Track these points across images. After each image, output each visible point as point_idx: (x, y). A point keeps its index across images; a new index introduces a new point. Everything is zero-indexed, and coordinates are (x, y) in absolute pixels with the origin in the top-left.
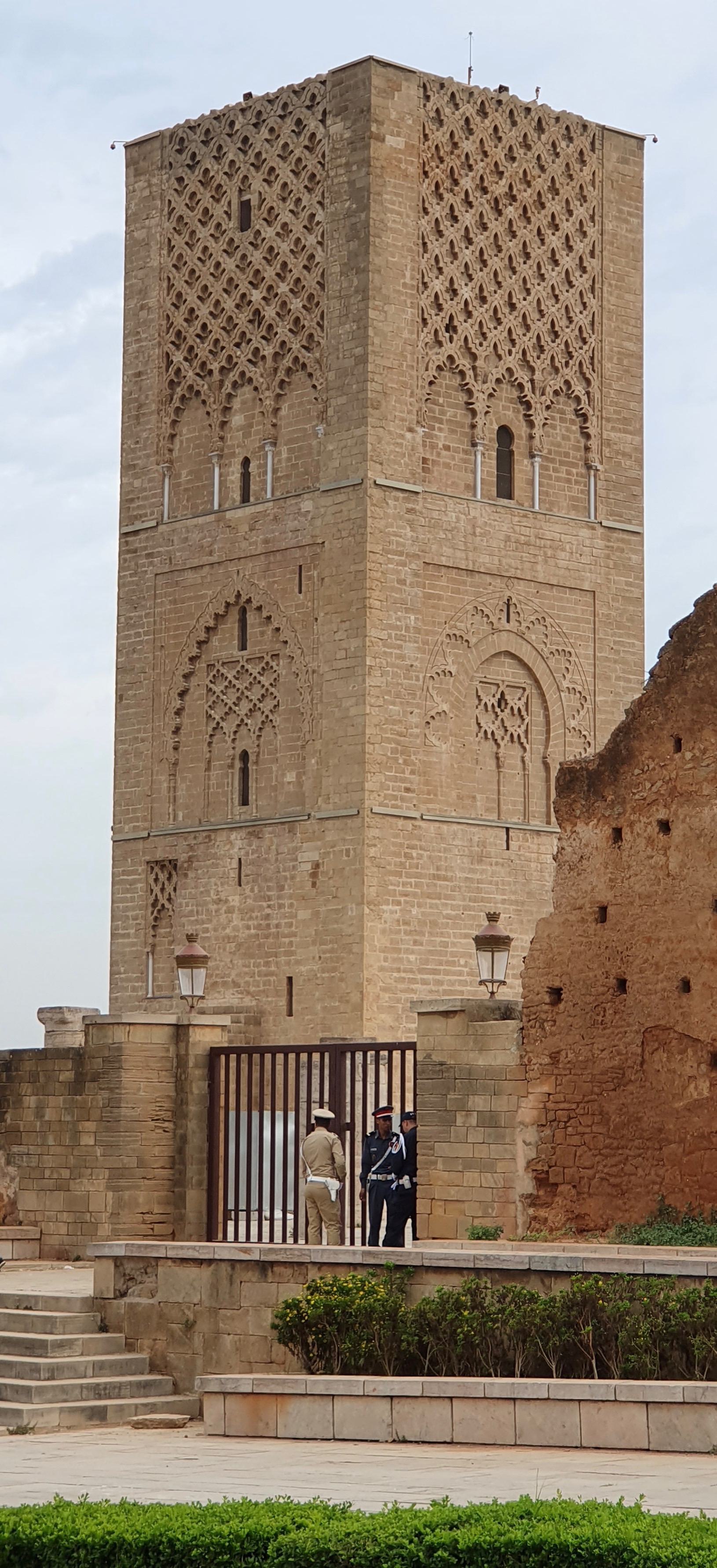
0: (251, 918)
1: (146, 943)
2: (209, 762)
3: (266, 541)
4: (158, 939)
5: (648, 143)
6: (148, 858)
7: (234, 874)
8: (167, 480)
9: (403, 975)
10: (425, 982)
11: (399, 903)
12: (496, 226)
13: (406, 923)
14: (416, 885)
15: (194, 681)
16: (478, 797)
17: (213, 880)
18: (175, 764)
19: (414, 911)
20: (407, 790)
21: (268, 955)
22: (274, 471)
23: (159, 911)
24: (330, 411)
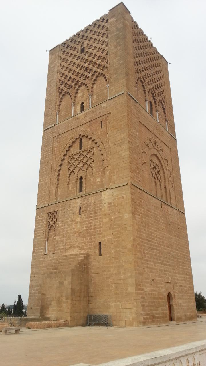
0: (84, 224)
1: (45, 237)
2: (69, 182)
3: (90, 118)
4: (50, 236)
5: (168, 64)
6: (47, 212)
7: (78, 212)
8: (57, 115)
9: (142, 240)
11: (140, 216)
13: (142, 223)
15: (64, 161)
16: (153, 192)
17: (70, 215)
18: (58, 184)
19: (144, 219)
20: (140, 181)
21: (91, 236)
22: (92, 102)
23: (51, 227)
24: (111, 80)
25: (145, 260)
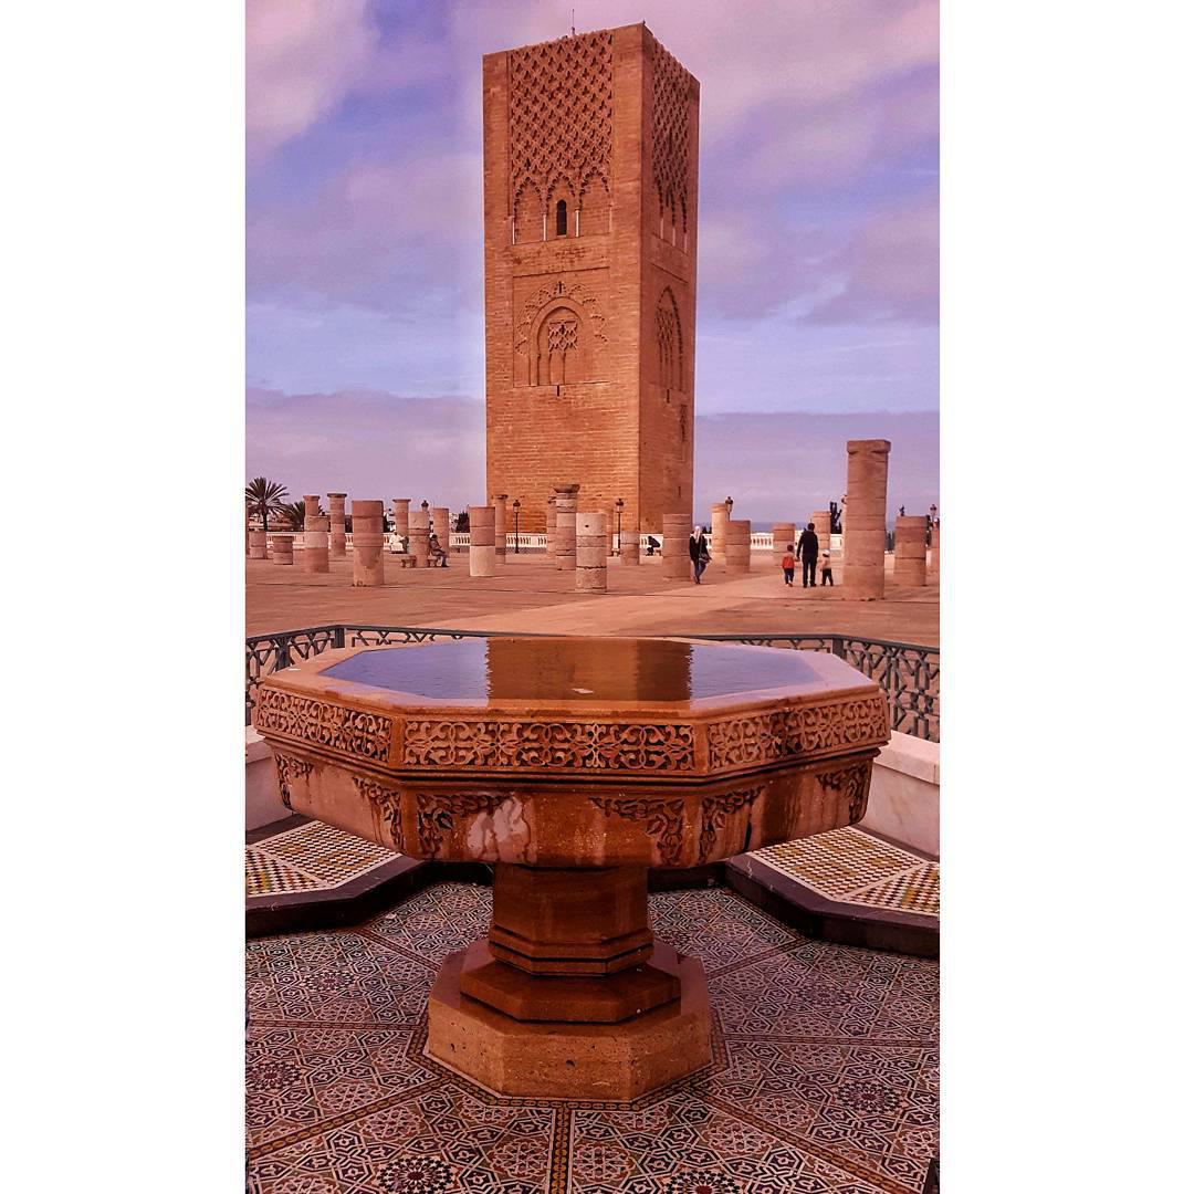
12: (552, 106)
19: (510, 428)
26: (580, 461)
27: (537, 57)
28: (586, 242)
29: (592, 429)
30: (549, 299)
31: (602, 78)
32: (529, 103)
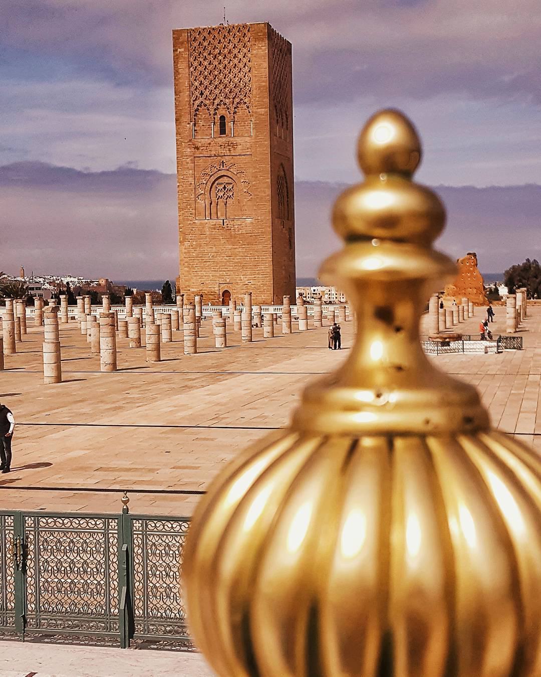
10: (198, 260)
11: (189, 241)
14: (195, 237)
25: (194, 271)
26: (239, 262)
27: (206, 34)
28: (238, 140)
29: (244, 245)
30: (216, 170)
31: (245, 50)
32: (201, 60)
